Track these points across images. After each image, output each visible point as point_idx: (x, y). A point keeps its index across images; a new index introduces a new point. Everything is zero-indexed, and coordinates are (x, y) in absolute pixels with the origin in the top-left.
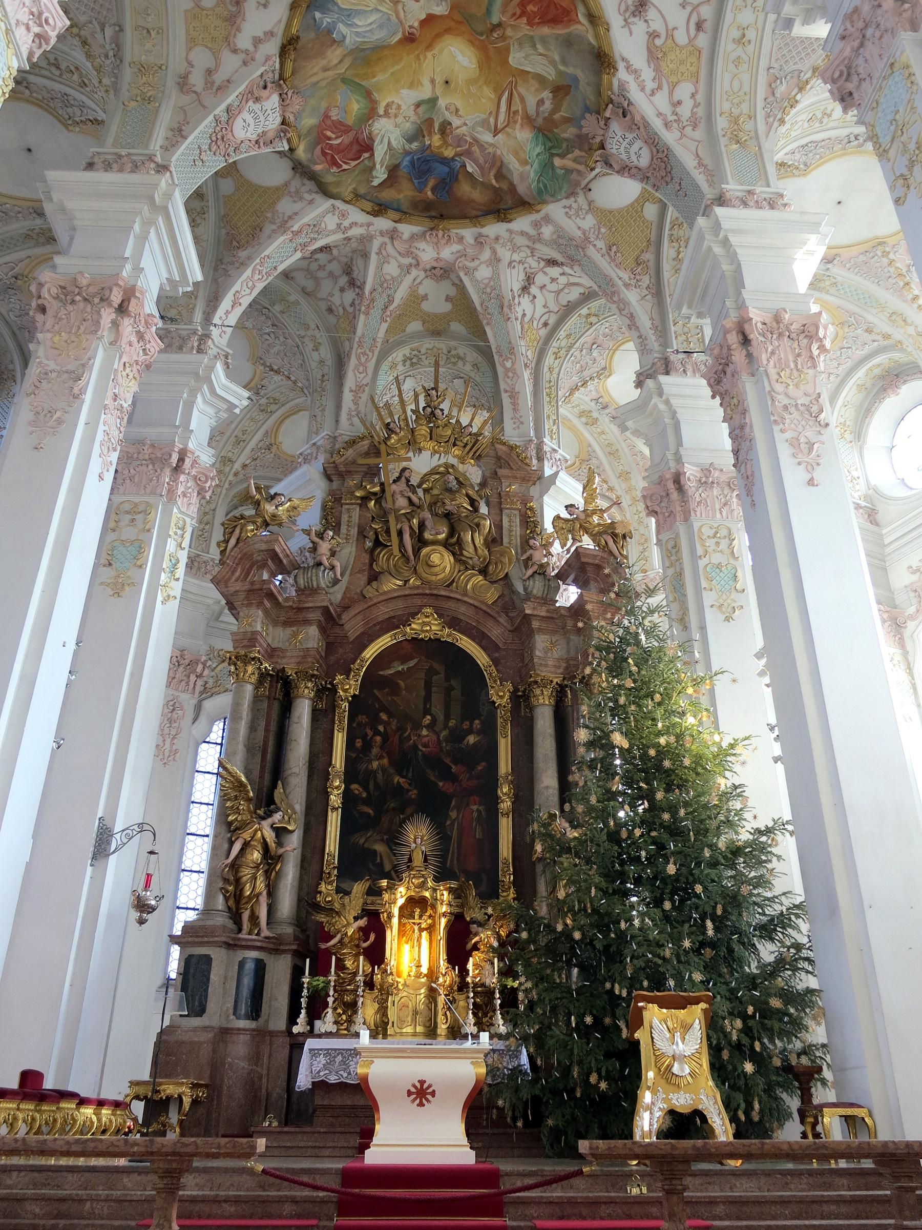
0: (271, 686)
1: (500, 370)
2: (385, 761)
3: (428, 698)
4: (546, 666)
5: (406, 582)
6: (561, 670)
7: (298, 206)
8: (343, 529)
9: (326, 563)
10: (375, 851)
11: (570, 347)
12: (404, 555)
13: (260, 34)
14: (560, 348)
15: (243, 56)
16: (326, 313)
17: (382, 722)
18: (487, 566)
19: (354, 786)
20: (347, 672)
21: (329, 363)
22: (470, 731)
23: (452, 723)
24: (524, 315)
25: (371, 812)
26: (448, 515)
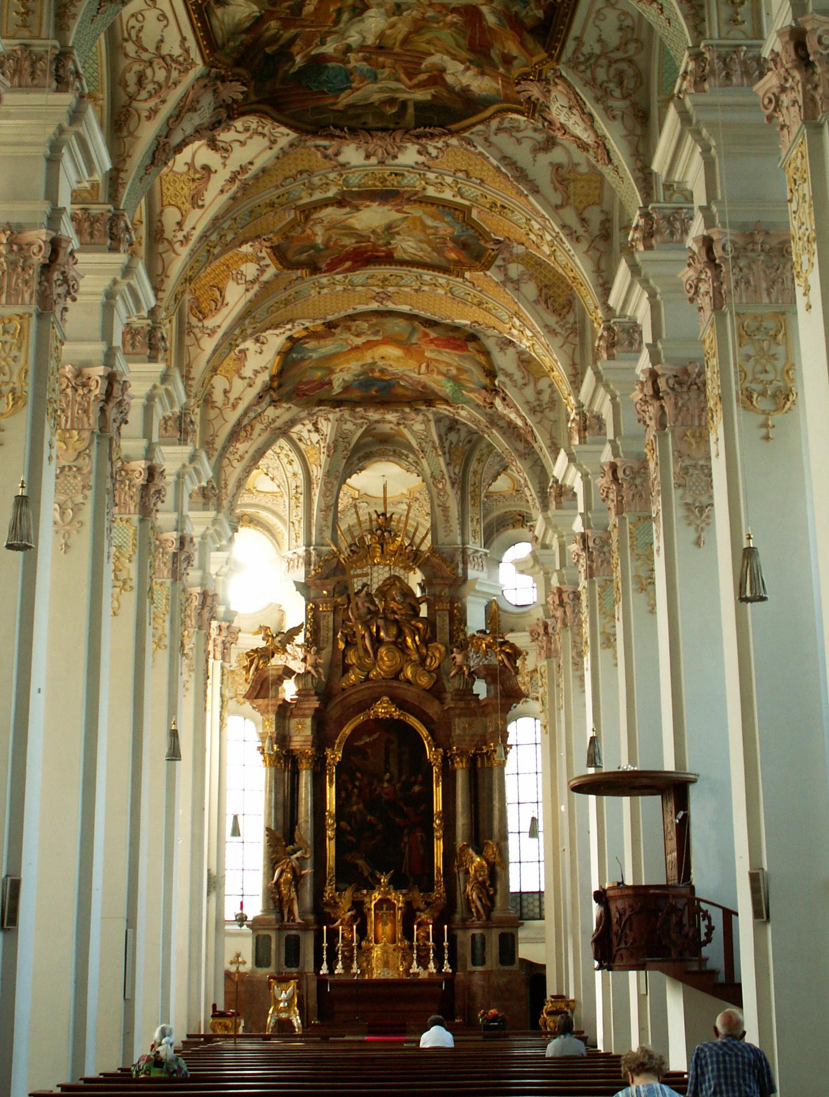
0: (285, 762)
1: (434, 490)
2: (361, 806)
3: (387, 762)
4: (464, 740)
5: (369, 672)
6: (474, 743)
7: (278, 412)
8: (323, 633)
9: (313, 672)
10: (357, 865)
11: (490, 452)
12: (366, 650)
13: (258, 368)
14: (482, 455)
15: (247, 381)
16: (298, 441)
17: (357, 779)
18: (425, 659)
19: (343, 824)
20: (332, 746)
21: (301, 477)
22: (415, 783)
23: (404, 778)
24: (451, 443)
25: (354, 840)
26: (396, 621)
